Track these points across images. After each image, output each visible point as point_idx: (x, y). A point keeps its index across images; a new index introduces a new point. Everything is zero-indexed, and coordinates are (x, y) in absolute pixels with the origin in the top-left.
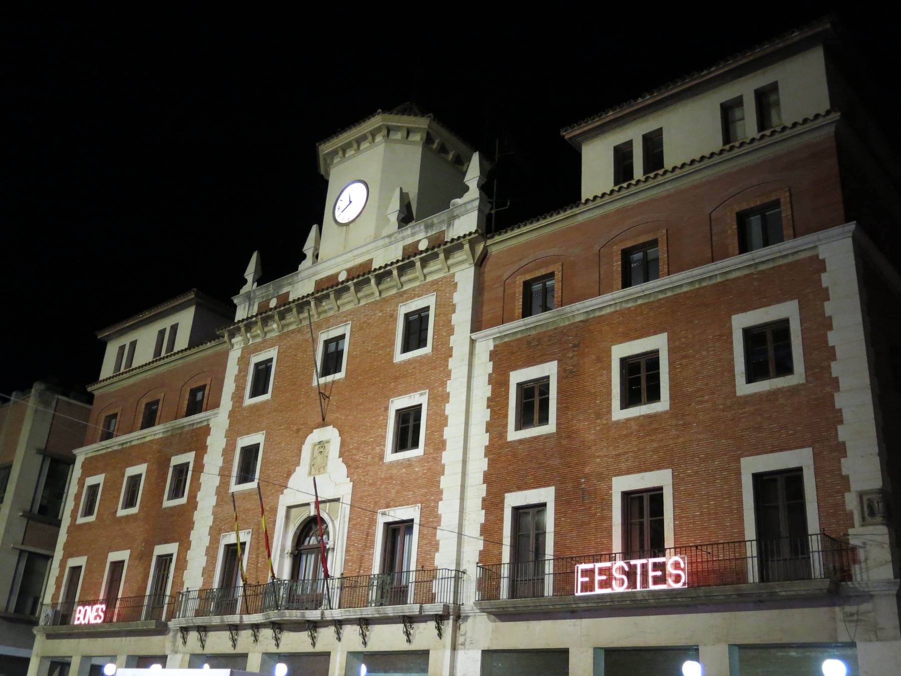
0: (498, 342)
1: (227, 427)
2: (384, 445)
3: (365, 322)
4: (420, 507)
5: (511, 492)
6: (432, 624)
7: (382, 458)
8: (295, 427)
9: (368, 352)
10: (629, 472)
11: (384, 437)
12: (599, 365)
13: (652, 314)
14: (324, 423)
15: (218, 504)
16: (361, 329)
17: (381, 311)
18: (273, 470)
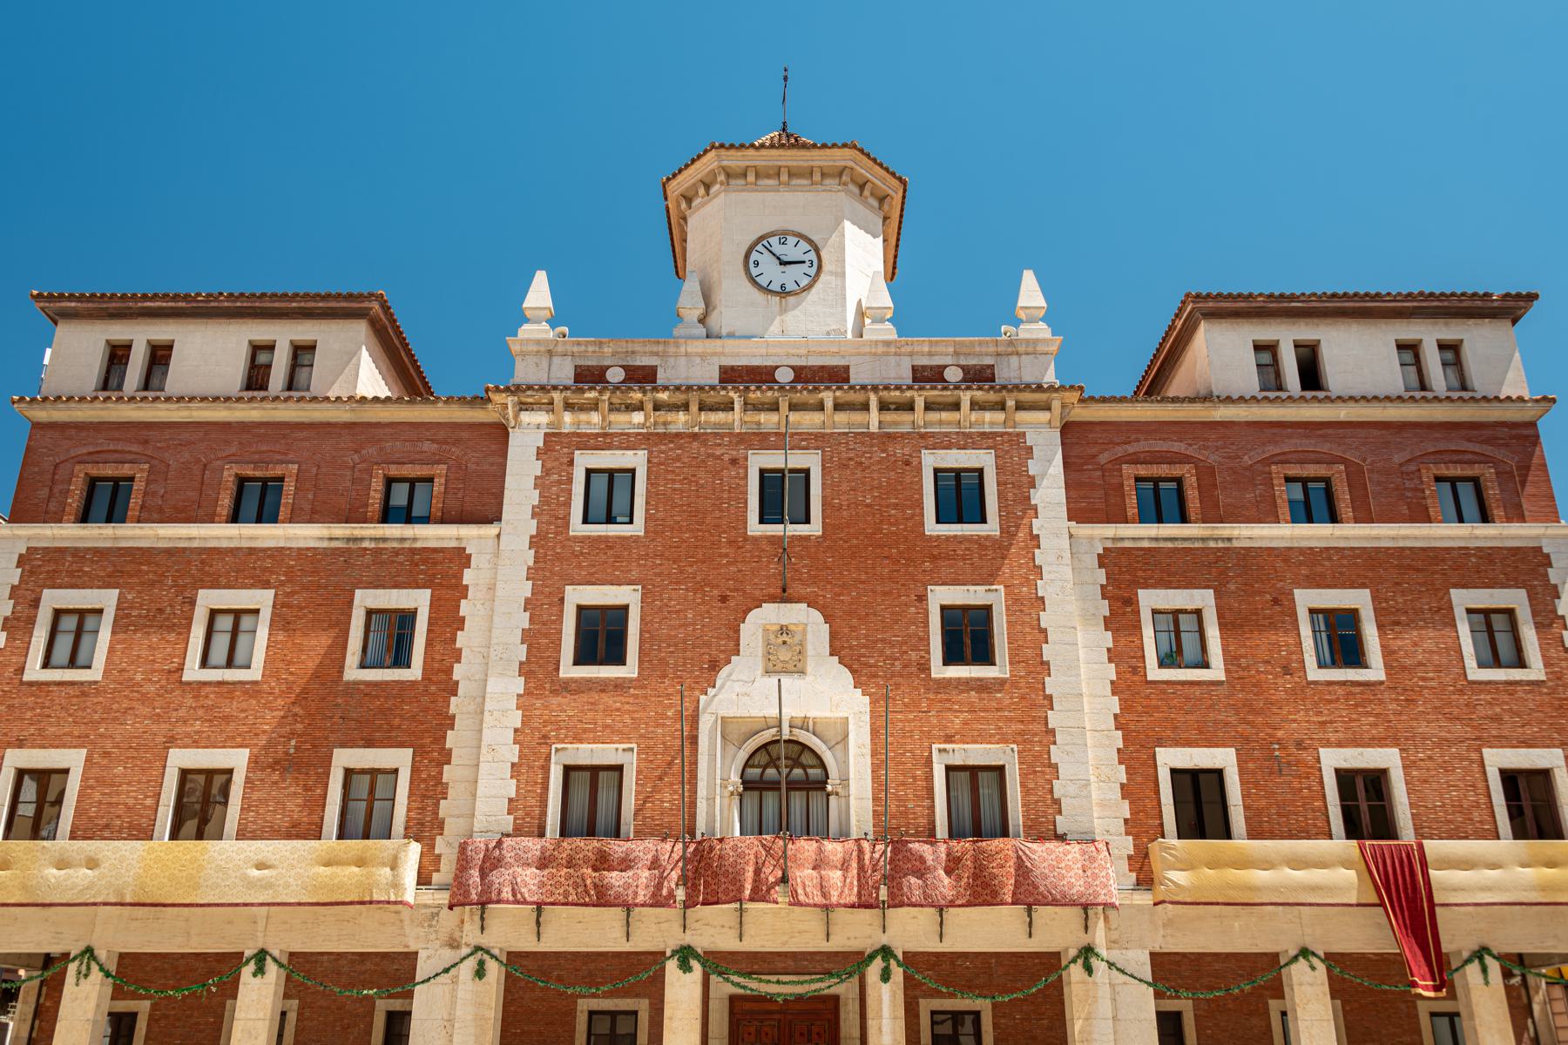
0: (1109, 544)
1: (531, 563)
2: (928, 652)
3: (850, 459)
4: (1016, 749)
5: (1165, 747)
6: (1078, 911)
7: (925, 667)
8: (716, 592)
9: (868, 506)
10: (1340, 744)
11: (926, 640)
12: (1278, 608)
13: (1345, 562)
14: (784, 596)
15: (528, 693)
16: (843, 466)
17: (883, 451)
18: (672, 652)
